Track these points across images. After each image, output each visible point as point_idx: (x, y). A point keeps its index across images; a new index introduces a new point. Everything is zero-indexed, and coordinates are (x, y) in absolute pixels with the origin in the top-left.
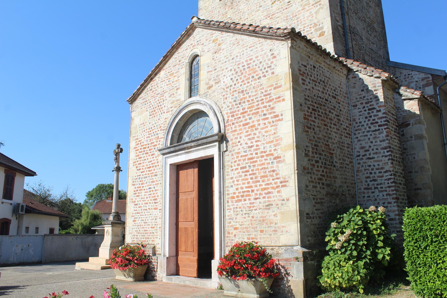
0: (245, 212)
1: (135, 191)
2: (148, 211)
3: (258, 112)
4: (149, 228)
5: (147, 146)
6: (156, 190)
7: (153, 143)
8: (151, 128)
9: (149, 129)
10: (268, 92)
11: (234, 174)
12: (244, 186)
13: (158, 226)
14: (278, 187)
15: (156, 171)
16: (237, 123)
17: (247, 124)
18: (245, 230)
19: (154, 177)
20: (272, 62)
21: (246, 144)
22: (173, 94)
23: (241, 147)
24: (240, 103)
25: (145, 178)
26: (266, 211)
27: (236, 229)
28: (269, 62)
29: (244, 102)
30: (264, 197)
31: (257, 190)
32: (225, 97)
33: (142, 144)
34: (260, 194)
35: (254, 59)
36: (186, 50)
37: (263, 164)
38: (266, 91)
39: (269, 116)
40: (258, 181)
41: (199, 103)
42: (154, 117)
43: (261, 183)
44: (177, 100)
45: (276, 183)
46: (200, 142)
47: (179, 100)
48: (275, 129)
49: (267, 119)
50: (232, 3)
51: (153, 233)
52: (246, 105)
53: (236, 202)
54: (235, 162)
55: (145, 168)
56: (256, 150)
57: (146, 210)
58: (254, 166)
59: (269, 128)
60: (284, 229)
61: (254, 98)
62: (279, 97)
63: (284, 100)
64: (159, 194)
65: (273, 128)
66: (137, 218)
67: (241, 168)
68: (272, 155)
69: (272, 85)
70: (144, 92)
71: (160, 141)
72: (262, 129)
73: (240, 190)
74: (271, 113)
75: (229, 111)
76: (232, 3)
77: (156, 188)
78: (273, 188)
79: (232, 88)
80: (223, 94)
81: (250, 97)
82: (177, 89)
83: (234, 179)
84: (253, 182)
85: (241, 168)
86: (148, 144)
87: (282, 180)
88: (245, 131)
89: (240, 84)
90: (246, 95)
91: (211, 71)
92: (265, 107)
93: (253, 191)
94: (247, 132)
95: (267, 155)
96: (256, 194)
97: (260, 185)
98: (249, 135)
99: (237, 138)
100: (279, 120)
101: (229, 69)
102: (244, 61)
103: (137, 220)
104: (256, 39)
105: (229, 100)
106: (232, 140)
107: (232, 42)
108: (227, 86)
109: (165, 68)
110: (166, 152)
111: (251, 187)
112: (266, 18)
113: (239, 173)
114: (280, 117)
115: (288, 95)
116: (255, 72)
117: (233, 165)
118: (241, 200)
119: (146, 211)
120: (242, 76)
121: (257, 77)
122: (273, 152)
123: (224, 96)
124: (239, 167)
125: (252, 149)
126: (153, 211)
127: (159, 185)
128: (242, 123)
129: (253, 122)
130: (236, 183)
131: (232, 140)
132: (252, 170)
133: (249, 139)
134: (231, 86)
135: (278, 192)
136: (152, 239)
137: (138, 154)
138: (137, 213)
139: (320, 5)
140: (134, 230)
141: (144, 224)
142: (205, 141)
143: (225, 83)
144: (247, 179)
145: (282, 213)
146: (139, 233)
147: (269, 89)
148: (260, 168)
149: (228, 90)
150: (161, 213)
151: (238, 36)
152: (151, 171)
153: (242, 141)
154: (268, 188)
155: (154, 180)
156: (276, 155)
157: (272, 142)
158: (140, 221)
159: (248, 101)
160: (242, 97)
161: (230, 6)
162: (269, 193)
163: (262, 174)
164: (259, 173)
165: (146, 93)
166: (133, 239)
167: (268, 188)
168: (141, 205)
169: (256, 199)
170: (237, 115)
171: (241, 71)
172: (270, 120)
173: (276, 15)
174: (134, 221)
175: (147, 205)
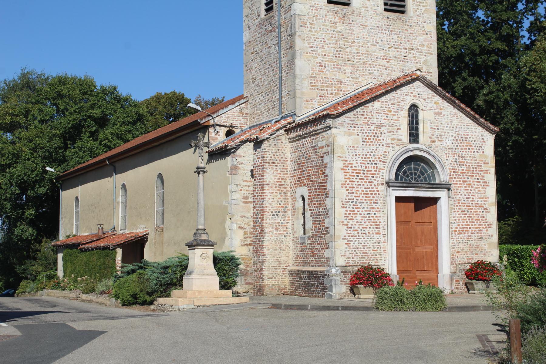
0: (464, 241)
1: (346, 214)
2: (368, 235)
3: (473, 176)
4: (369, 251)
5: (362, 172)
6: (376, 217)
7: (371, 171)
8: (366, 155)
9: (363, 155)
10: (480, 164)
11: (456, 214)
12: (464, 224)
13: (382, 249)
14: (486, 227)
15: (376, 198)
16: (458, 178)
17: (466, 181)
18: (465, 253)
19: (374, 205)
20: (482, 144)
21: (465, 195)
22: (393, 132)
23: (461, 197)
24: (460, 165)
25: (360, 203)
26: (479, 242)
27: (458, 252)
28: (481, 144)
29: (463, 165)
30: (478, 233)
31: (473, 228)
32: (448, 155)
33: (354, 168)
34: (475, 231)
35: (470, 136)
36: (406, 95)
37: (477, 211)
38: (478, 163)
39: (481, 181)
40: (474, 222)
41: (420, 148)
42: (370, 145)
43: (475, 223)
44: (398, 140)
45: (485, 225)
46: (434, 186)
47: (401, 140)
48: (485, 191)
49: (479, 182)
50: (344, 17)
51: (376, 255)
52: (465, 168)
53: (458, 234)
54: (457, 206)
55: (361, 194)
56: (472, 201)
57: (365, 233)
58: (471, 212)
59: (481, 189)
60: (490, 253)
61: (470, 164)
62: (487, 171)
63: (490, 173)
64: (382, 221)
65: (483, 189)
66: (352, 241)
67: (462, 211)
68: (483, 207)
69: (482, 161)
70: (352, 113)
71: (379, 171)
72: (476, 188)
73: (461, 226)
74: (482, 179)
75: (451, 168)
76: (344, 17)
77: (376, 215)
78: (483, 228)
79: (453, 150)
80: (446, 152)
81: (467, 162)
82: (398, 129)
83: (456, 218)
84: (470, 222)
85: (462, 211)
86: (364, 171)
87: (488, 223)
88: (464, 186)
89: (459, 150)
90: (464, 160)
91: (434, 129)
92: (478, 174)
93: (470, 228)
94: (466, 187)
95: (480, 206)
96: (472, 230)
97: (475, 225)
98: (467, 190)
99: (457, 189)
100: (487, 185)
101: (451, 134)
102: (462, 133)
103: (351, 243)
104: (471, 122)
105: (451, 158)
106: (454, 190)
107: (452, 113)
108: (449, 147)
109: (379, 100)
110: (389, 184)
111: (469, 225)
112: (383, 59)
113: (460, 214)
114: (488, 184)
115: (493, 171)
116: (471, 146)
117: (455, 208)
118: (461, 233)
119: (364, 235)
120: (461, 145)
121: (472, 151)
122: (483, 205)
123: (446, 154)
124: (460, 210)
125: (469, 200)
126: (375, 235)
127: (381, 212)
128: (461, 180)
129: (470, 181)
130: (457, 221)
131: (454, 190)
132: (470, 214)
133: (467, 193)
134: (452, 149)
135: (487, 230)
136: (375, 261)
137: (348, 176)
138: (352, 236)
139: (431, 76)
140: (347, 253)
141: (362, 247)
142: (439, 186)
143: (448, 144)
144: (466, 220)
145: (489, 244)
146: (355, 255)
147: (480, 162)
148: (475, 213)
149: (450, 150)
150: (386, 238)
151: (458, 112)
152: (369, 197)
153: (462, 193)
154: (480, 228)
155: (374, 206)
156: (485, 207)
157: (483, 198)
158: (356, 244)
159: (466, 165)
160: (461, 160)
161: (341, 18)
162: (481, 230)
163: (476, 218)
164: (474, 217)
165: (355, 115)
166: (347, 262)
167: (480, 228)
168: (356, 228)
169: (472, 233)
170: (457, 172)
171: (460, 140)
172: (481, 184)
173: (393, 61)
174: (346, 244)
175: (366, 230)
